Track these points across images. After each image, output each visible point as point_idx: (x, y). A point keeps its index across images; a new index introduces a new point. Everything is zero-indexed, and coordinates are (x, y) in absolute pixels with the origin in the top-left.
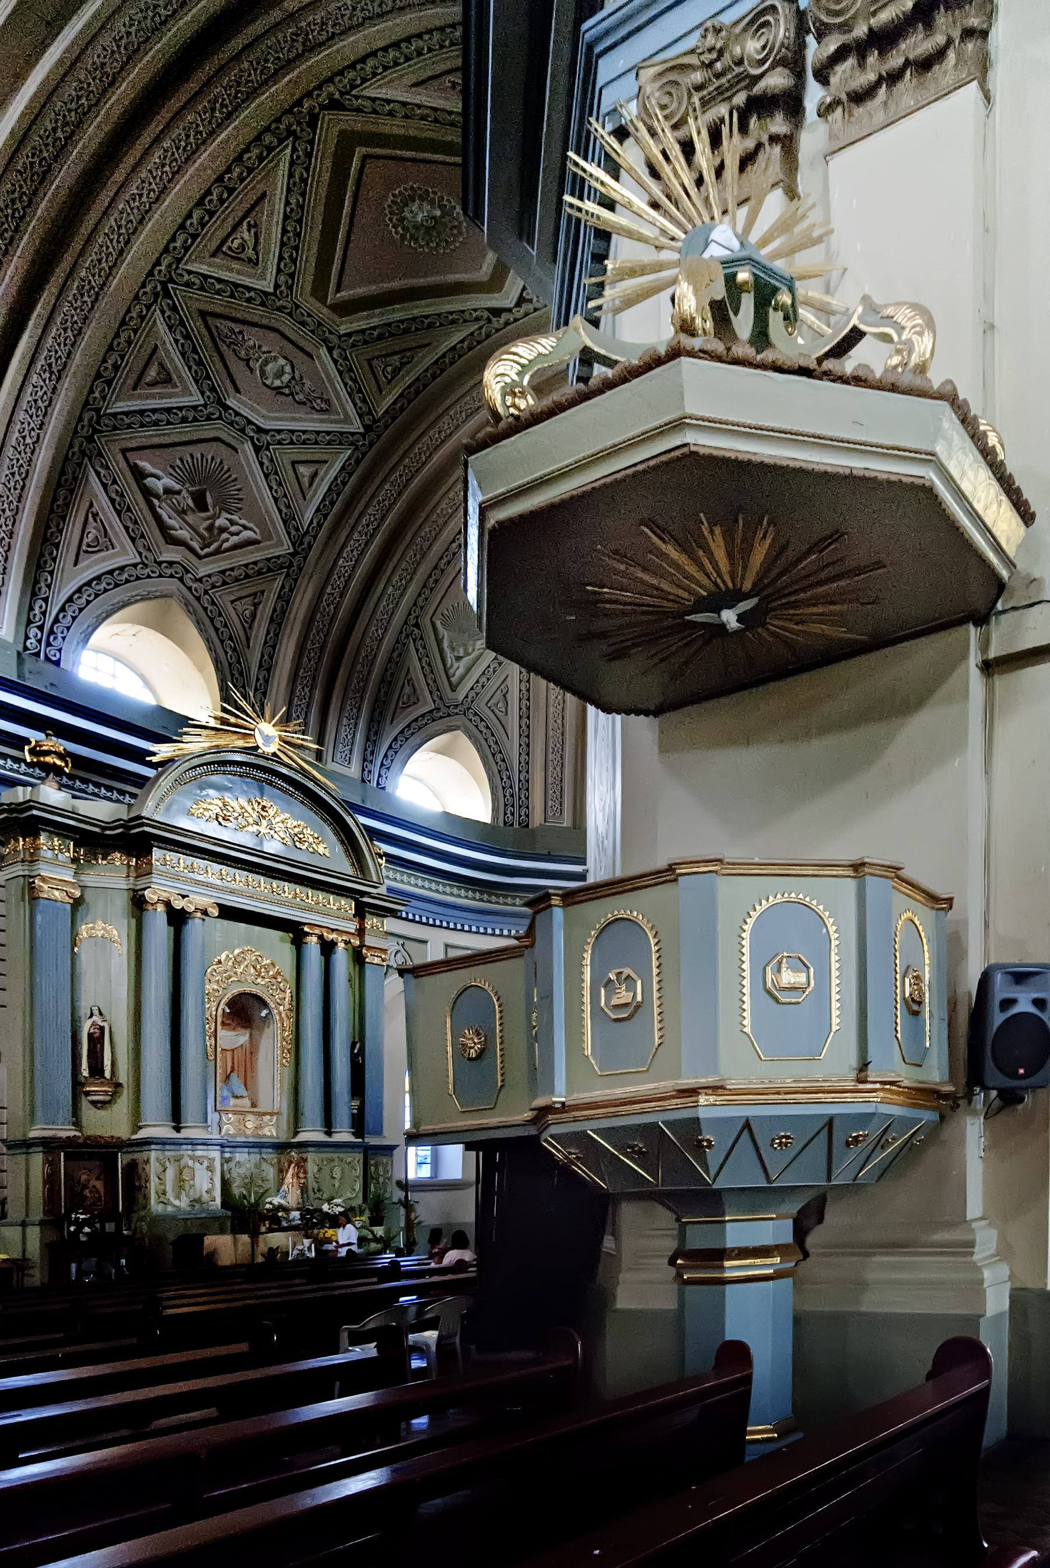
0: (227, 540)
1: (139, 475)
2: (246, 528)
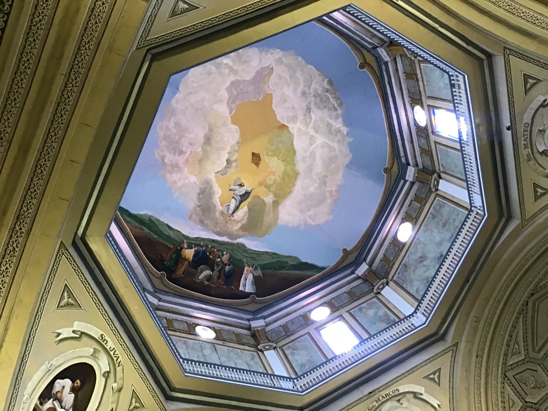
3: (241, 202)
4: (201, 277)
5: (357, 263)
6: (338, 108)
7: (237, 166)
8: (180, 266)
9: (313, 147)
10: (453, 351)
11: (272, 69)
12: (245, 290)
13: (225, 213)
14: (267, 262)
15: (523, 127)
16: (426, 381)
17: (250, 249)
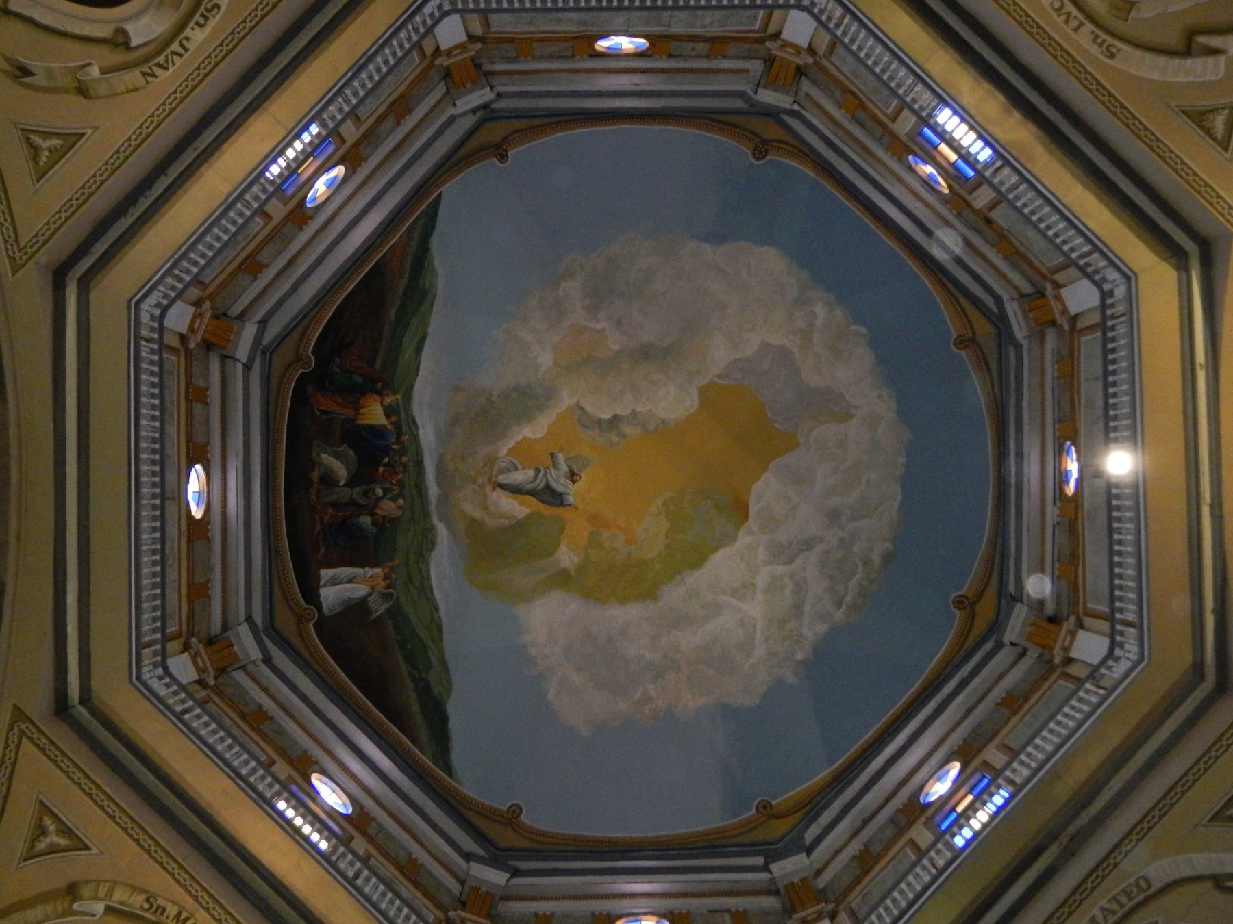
3: (532, 493)
4: (326, 459)
5: (497, 856)
6: (844, 607)
7: (611, 444)
8: (340, 400)
9: (729, 599)
11: (850, 416)
12: (325, 585)
13: (496, 468)
14: (413, 619)
15: (1133, 880)
17: (428, 565)
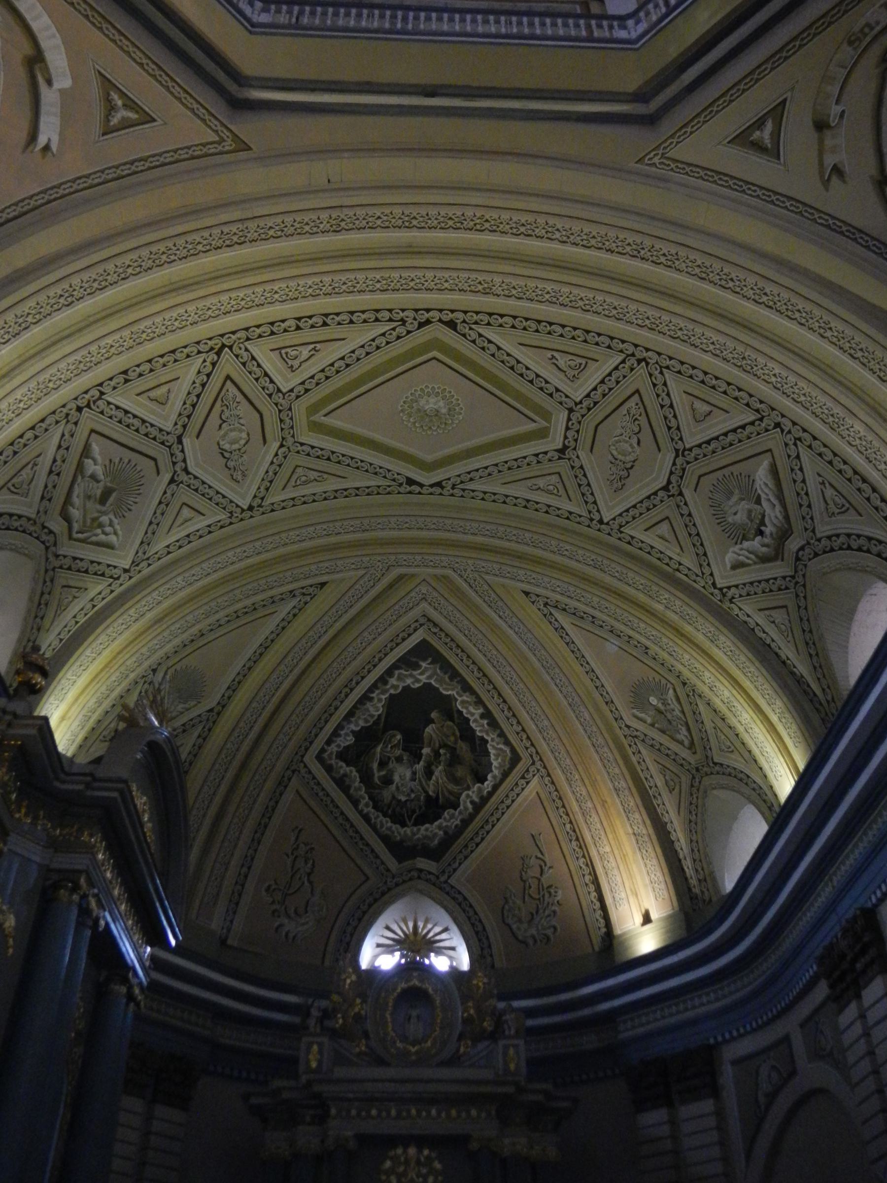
0: (96, 535)
1: (86, 451)
2: (115, 533)
10: (219, 143)
16: (94, 90)
